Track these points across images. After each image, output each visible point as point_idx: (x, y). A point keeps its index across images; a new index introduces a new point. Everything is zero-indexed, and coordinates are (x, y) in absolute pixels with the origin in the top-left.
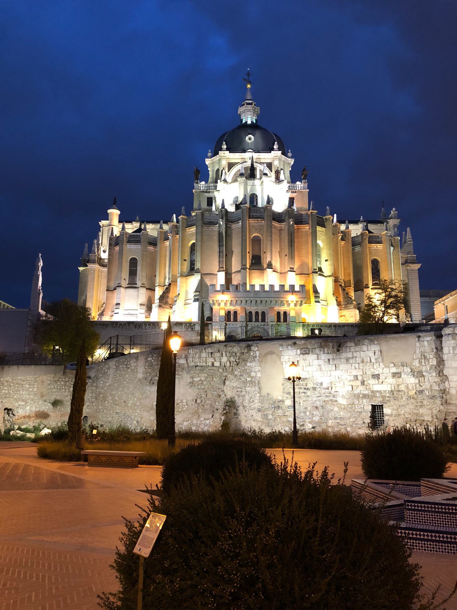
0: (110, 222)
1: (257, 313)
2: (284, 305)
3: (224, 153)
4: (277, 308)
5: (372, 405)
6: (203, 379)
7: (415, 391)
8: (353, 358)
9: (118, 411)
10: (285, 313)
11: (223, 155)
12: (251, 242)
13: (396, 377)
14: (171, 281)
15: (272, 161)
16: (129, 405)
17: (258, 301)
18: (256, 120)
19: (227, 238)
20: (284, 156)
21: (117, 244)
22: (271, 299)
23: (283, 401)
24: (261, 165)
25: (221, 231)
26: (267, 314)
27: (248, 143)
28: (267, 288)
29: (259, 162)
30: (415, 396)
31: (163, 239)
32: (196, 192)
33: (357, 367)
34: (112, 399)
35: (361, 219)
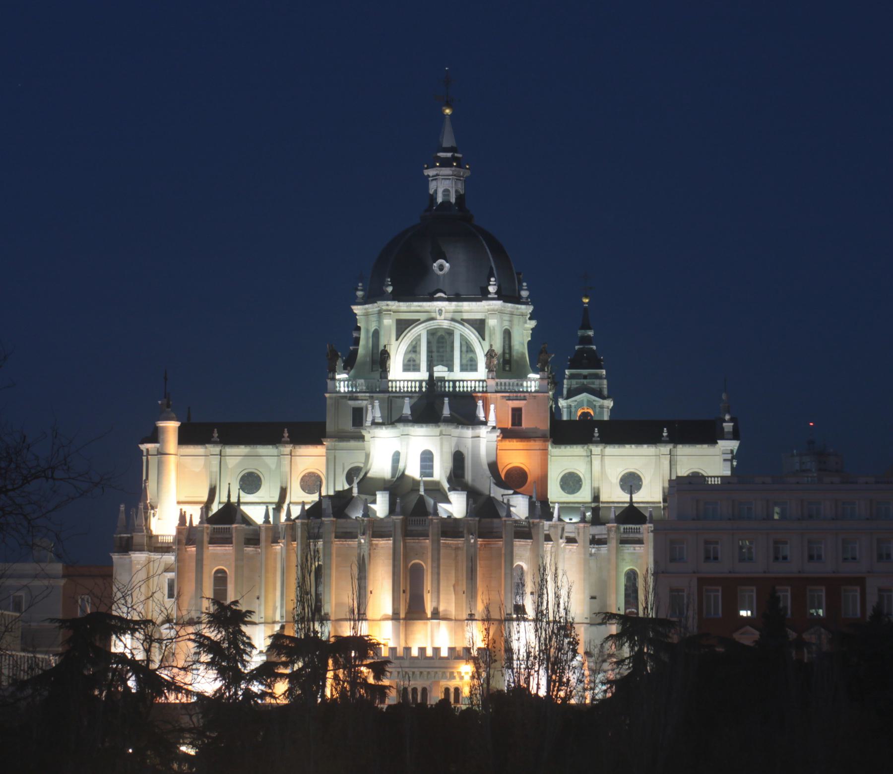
0: (162, 447)
2: (454, 678)
3: (387, 305)
4: (444, 683)
10: (457, 690)
11: (384, 308)
12: (408, 574)
14: (286, 622)
15: (486, 316)
17: (416, 673)
18: (459, 197)
20: (510, 305)
21: (190, 541)
22: (435, 670)
24: (463, 325)
25: (362, 554)
26: (431, 691)
27: (438, 276)
28: (429, 653)
29: (459, 320)
31: (270, 540)
32: (331, 398)
35: (665, 434)
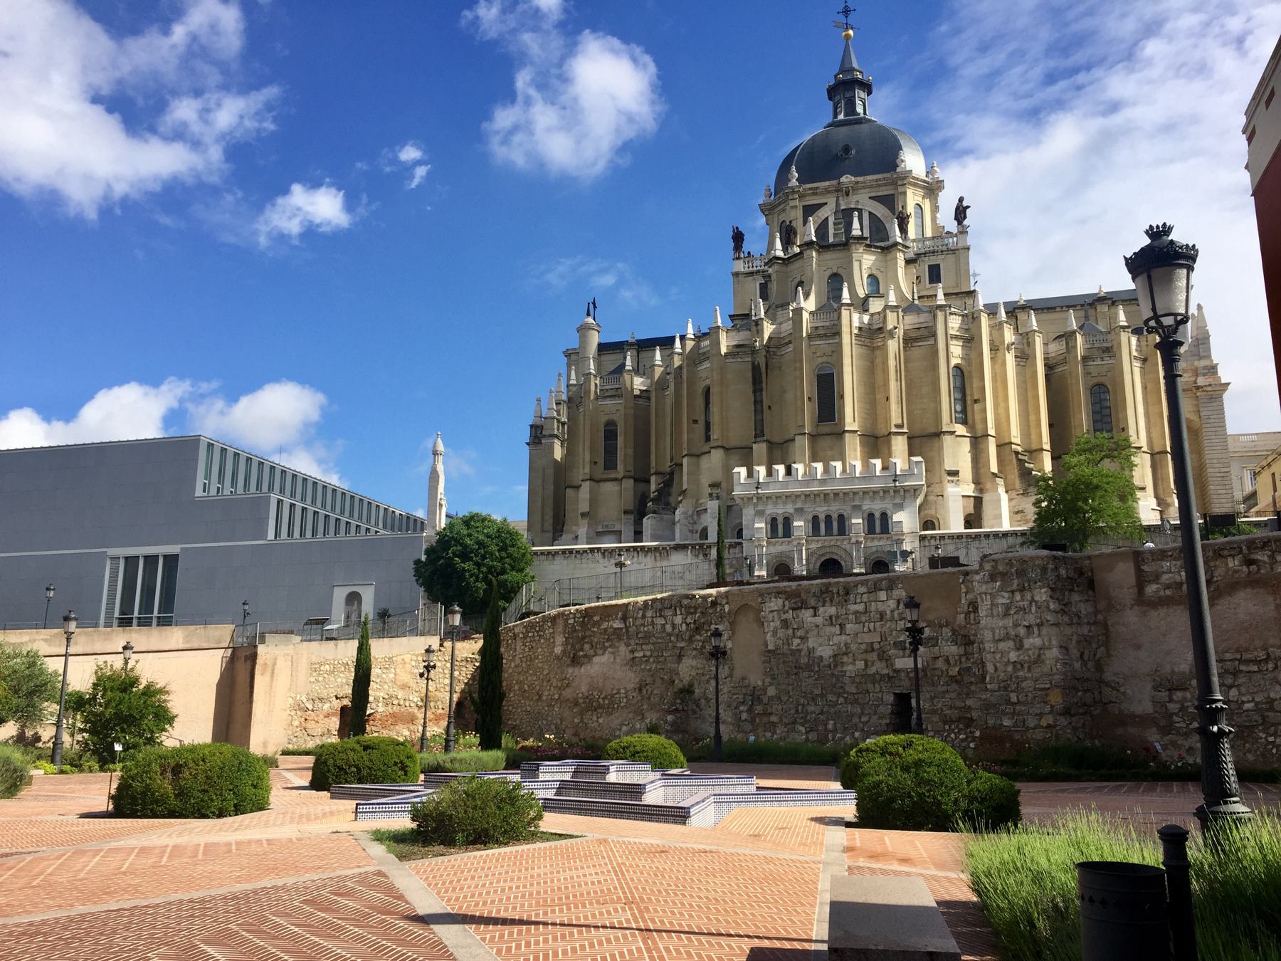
1: (828, 518)
5: (895, 694)
6: (648, 653)
7: (957, 669)
8: (866, 612)
9: (529, 708)
13: (930, 645)
16: (544, 698)
19: (769, 377)
23: (765, 690)
30: (959, 678)
33: (872, 628)
34: (520, 689)
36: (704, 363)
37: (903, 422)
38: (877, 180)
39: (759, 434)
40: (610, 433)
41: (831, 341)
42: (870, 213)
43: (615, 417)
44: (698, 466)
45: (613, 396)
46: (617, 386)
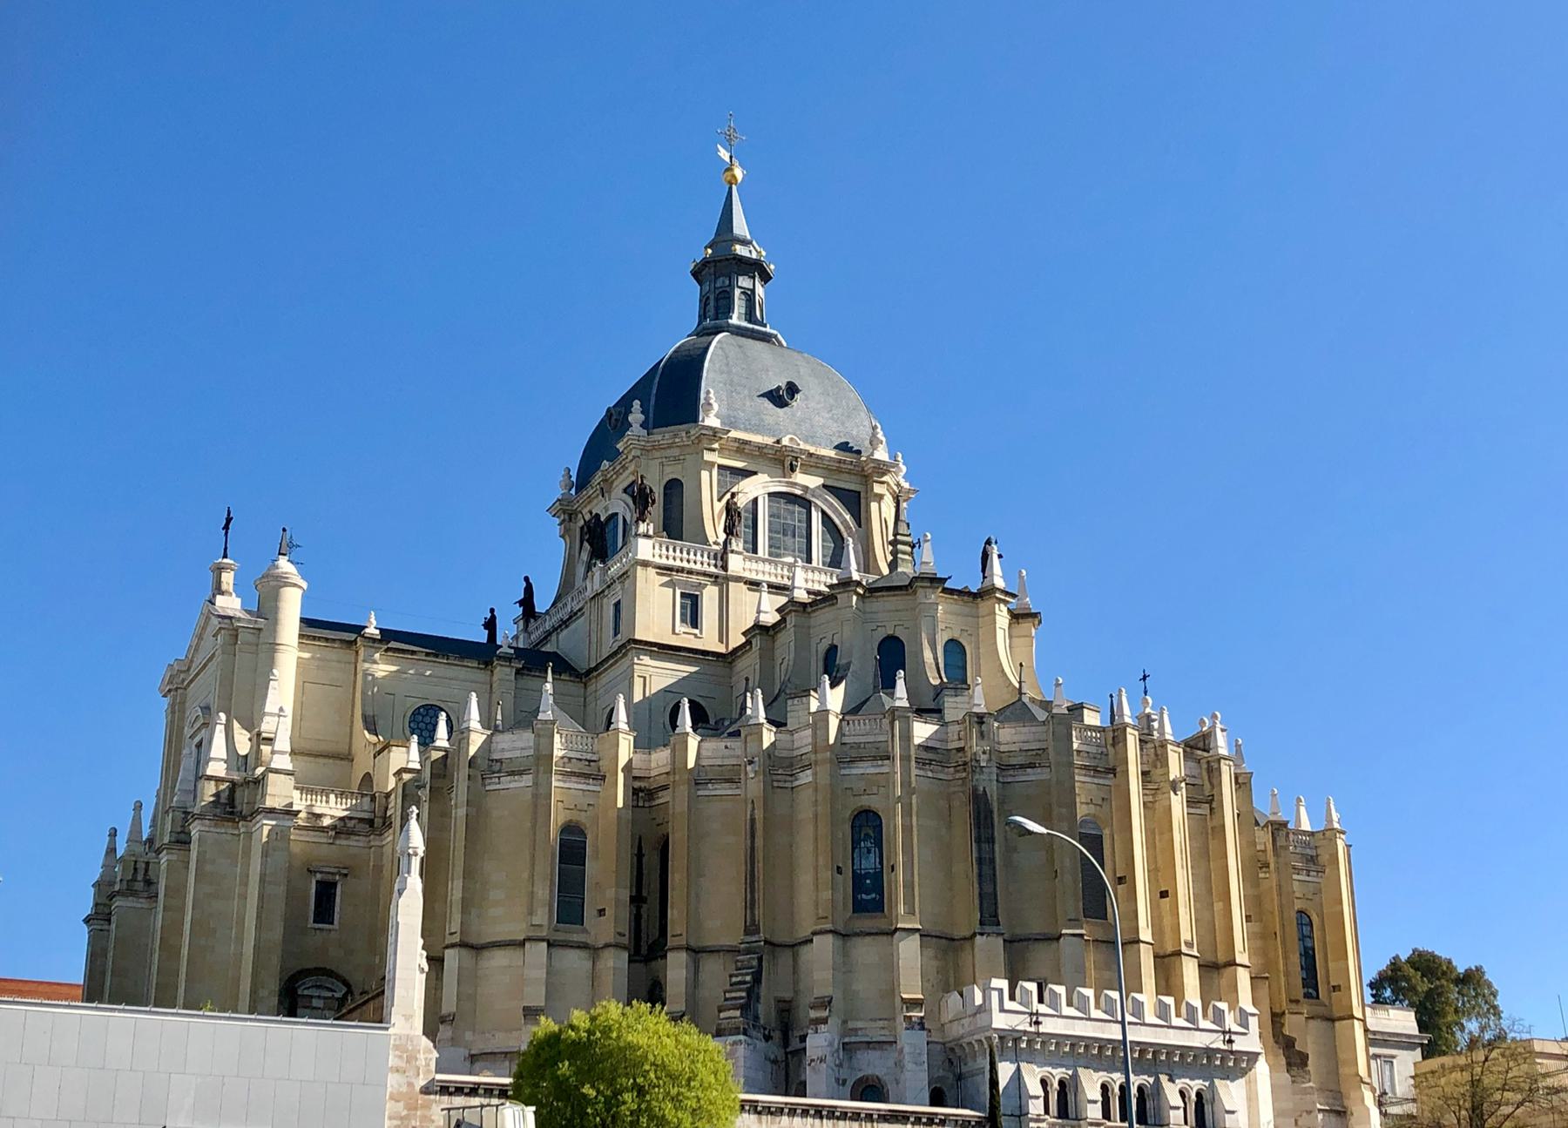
1: (1124, 1089)
36: (861, 764)
37: (1192, 940)
38: (840, 461)
39: (989, 918)
40: (572, 849)
41: (1101, 781)
42: (824, 513)
43: (582, 818)
44: (845, 953)
45: (586, 776)
46: (589, 756)
